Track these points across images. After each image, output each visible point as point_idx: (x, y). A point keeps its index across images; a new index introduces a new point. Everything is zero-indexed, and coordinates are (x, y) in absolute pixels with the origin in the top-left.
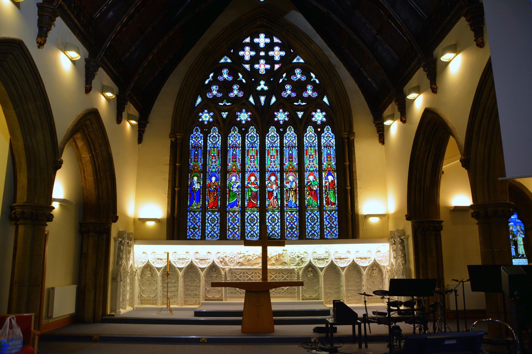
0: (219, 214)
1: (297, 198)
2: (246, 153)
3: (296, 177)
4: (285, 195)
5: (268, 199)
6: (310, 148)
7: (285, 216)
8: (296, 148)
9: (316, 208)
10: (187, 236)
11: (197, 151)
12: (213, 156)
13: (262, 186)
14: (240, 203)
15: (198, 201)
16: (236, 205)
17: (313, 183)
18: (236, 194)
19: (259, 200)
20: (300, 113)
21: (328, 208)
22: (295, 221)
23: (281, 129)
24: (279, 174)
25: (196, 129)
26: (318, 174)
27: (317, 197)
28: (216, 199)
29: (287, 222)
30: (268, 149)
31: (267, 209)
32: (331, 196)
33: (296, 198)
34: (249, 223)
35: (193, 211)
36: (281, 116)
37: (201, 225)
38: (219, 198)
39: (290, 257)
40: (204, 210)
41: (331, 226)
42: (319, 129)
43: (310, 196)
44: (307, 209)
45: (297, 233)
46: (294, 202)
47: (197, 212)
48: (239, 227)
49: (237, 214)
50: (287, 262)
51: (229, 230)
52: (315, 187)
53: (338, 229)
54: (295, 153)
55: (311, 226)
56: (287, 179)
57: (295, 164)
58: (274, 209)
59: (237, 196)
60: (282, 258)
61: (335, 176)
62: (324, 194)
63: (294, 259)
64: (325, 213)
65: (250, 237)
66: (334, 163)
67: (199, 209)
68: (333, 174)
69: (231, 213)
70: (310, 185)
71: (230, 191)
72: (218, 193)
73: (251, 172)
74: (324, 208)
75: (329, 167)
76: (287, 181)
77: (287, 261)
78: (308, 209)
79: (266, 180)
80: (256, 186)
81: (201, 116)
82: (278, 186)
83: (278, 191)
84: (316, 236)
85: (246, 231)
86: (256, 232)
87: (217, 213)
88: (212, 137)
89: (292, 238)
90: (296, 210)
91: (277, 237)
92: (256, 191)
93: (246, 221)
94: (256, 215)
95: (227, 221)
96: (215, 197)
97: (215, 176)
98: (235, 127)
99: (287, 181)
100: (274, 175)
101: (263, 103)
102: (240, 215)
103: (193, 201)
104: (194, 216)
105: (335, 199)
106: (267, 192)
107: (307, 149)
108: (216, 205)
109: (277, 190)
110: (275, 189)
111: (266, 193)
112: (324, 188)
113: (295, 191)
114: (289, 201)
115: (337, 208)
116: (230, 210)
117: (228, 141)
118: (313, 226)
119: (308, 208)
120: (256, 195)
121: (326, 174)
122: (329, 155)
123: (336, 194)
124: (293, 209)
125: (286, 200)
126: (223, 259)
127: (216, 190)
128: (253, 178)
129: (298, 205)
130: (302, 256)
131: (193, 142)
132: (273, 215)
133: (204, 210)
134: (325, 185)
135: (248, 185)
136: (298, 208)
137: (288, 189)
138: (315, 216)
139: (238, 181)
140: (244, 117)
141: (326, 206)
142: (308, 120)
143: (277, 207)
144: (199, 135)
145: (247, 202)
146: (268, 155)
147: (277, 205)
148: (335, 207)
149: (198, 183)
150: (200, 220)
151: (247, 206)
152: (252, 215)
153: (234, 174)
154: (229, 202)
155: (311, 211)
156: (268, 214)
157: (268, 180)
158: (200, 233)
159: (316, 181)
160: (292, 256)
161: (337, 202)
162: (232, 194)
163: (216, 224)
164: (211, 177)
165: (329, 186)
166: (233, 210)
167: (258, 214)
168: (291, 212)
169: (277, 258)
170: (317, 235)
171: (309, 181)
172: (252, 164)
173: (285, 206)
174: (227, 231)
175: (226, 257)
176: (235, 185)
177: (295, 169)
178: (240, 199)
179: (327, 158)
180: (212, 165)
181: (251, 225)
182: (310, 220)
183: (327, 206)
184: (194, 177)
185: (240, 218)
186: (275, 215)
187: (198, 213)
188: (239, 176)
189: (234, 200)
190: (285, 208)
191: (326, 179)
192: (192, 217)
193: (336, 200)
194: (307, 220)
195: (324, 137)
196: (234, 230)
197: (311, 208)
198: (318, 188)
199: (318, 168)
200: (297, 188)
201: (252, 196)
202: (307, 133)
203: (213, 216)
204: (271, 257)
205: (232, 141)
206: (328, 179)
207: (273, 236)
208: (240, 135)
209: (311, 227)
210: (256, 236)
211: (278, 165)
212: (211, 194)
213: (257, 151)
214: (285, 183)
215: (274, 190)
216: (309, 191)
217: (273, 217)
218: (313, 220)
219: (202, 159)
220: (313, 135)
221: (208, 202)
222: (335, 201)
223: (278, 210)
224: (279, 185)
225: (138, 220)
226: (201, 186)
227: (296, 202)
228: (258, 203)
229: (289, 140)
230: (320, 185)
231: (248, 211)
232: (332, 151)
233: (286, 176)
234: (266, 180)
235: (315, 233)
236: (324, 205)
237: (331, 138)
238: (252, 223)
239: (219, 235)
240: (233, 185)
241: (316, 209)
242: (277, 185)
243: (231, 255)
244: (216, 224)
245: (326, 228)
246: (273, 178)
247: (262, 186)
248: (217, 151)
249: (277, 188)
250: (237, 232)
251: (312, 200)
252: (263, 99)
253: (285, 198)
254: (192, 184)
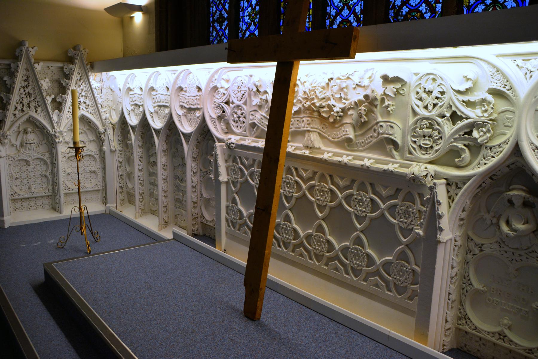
39: (415, 113)
50: (399, 141)
60: (380, 119)
63: (431, 126)
77: (404, 136)
126: (224, 112)
130: (474, 114)
160: (425, 113)
169: (361, 117)
175: (227, 103)
204: (343, 110)
225: (104, 11)
243: (239, 98)
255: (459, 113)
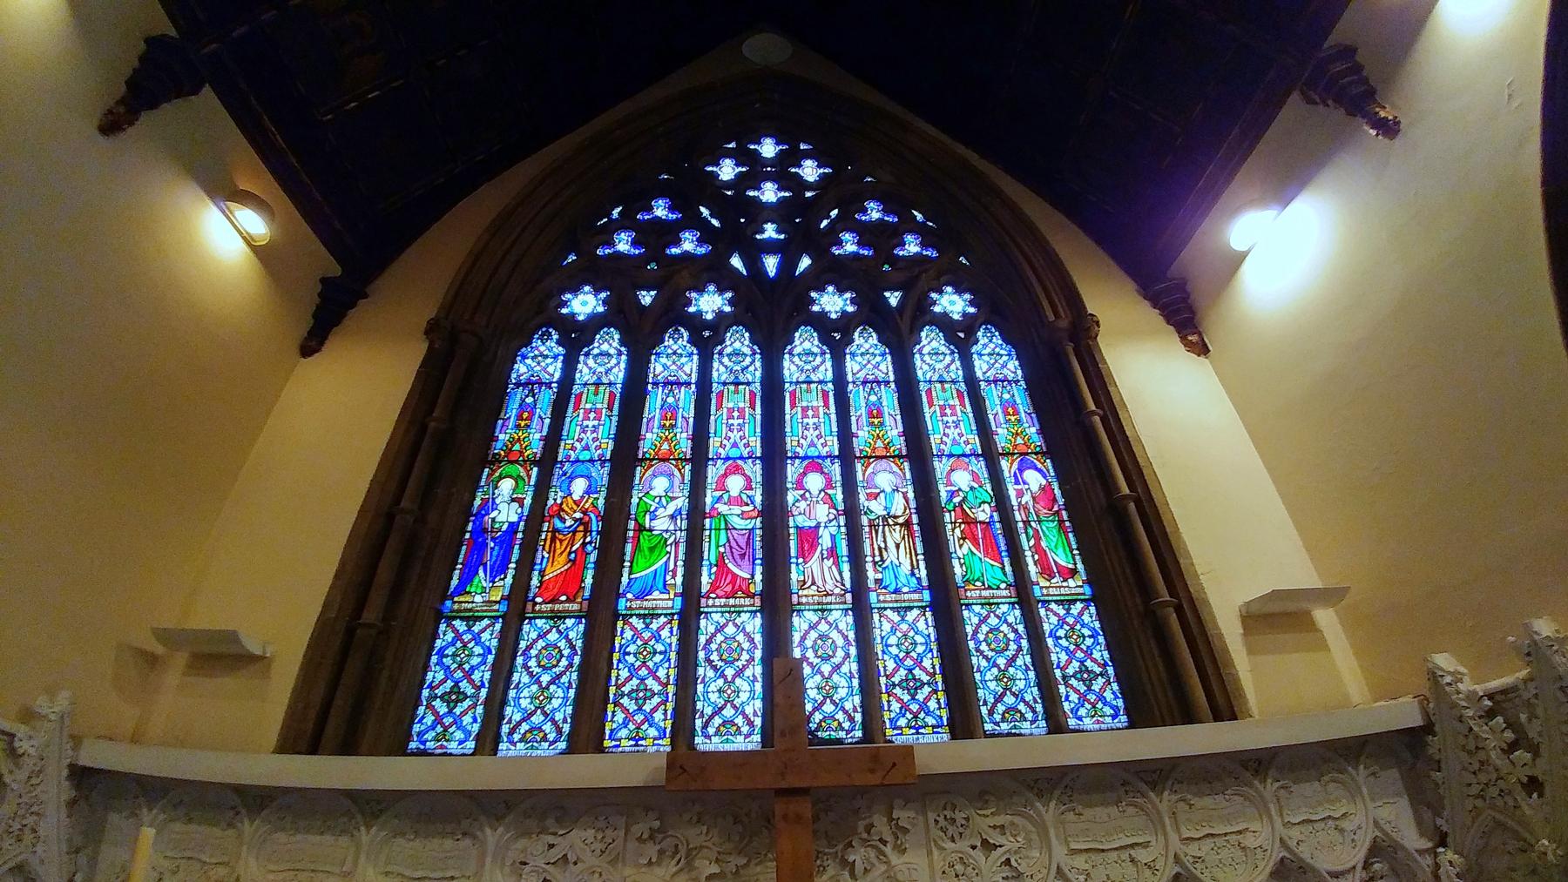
0: (582, 627)
1: (919, 552)
2: (714, 401)
3: (904, 474)
4: (868, 540)
5: (797, 558)
6: (938, 386)
7: (877, 632)
8: (893, 385)
9: (1005, 593)
10: (409, 738)
11: (534, 396)
12: (588, 412)
13: (774, 513)
14: (679, 579)
15: (499, 569)
16: (660, 585)
17: (970, 497)
18: (666, 540)
19: (761, 565)
20: (892, 293)
21: (1051, 591)
22: (920, 649)
23: (835, 336)
24: (837, 465)
25: (543, 335)
26: (983, 466)
27: (999, 547)
28: (577, 564)
29: (886, 657)
30: (791, 389)
31: (795, 599)
32: (1053, 545)
33: (912, 552)
34: (715, 668)
35: (467, 614)
36: (832, 302)
37: (490, 681)
38: (593, 557)
40: (517, 610)
41: (1083, 669)
42: (960, 336)
43: (968, 545)
44: (967, 598)
45: (940, 708)
46: (910, 568)
47: (482, 618)
48: (666, 685)
49: (665, 624)
51: (616, 704)
52: (983, 511)
53: (1118, 680)
54: (889, 399)
55: (995, 670)
56: (869, 483)
57: (895, 432)
58: (825, 600)
59: (668, 549)
61: (1048, 471)
62: (1023, 537)
64: (1042, 612)
65: (716, 734)
66: (1033, 430)
67: (496, 607)
68: (1039, 466)
69: (634, 620)
70: (960, 504)
71: (640, 529)
72: (588, 539)
73: (730, 462)
74: (1036, 588)
75: (1019, 441)
76: (868, 491)
78: (972, 598)
79: (788, 489)
80: (751, 508)
81: (569, 300)
82: (833, 506)
83: (839, 526)
84: (1025, 720)
85: (699, 705)
86: (749, 710)
87: (573, 620)
88: (597, 355)
89: (918, 733)
90: (922, 601)
91: (848, 732)
92: (750, 527)
93: (701, 655)
94: (749, 629)
95: (616, 656)
96: (573, 555)
97: (588, 477)
98: (679, 328)
99: (868, 491)
100: (819, 469)
101: (774, 271)
102: (675, 629)
103: (477, 573)
104: (467, 637)
105: (1070, 555)
106: (792, 531)
107: (930, 389)
108: (572, 591)
109: (834, 523)
110: (826, 519)
111: (789, 535)
112: (1017, 513)
113: (907, 524)
114: (887, 567)
115: (1087, 590)
116: (630, 608)
117: (652, 366)
118: (1006, 670)
119: (969, 594)
120: (748, 543)
121: (1015, 466)
122: (1009, 407)
123: (1071, 535)
124: (906, 597)
125: (875, 563)
127: (581, 528)
128: (735, 484)
129: (925, 583)
131: (523, 369)
132: (823, 627)
133: (517, 610)
134: (1020, 503)
135: (716, 506)
136: (926, 595)
137: (878, 518)
138: (1004, 628)
139: (675, 495)
140: (710, 303)
141: (1043, 583)
142: (919, 313)
143: (837, 591)
144: (551, 349)
145: (710, 575)
146: (793, 405)
147: (839, 584)
148: (1081, 587)
149: (513, 500)
150: (490, 658)
151: (710, 591)
152: (730, 630)
153: (664, 466)
154: (630, 574)
155: (982, 604)
156: (799, 623)
157: (796, 489)
158: (475, 720)
159: (979, 489)
161: (1080, 566)
162: (649, 541)
163: (562, 673)
164: (572, 478)
165: (1034, 507)
166: (645, 609)
167: (754, 624)
168: (903, 610)
170: (1029, 716)
171: (954, 489)
172: (735, 436)
173: (871, 584)
174: (610, 707)
176: (665, 508)
177: (894, 451)
178: (680, 563)
179: (1006, 413)
180: (580, 440)
181: (725, 677)
182: (989, 645)
183: (1048, 584)
184: (501, 478)
185: (673, 645)
186: (831, 625)
187: (486, 622)
188: (683, 476)
189: (654, 564)
190: (873, 597)
191: (1017, 482)
192: (453, 644)
193: (1078, 557)
194: (971, 644)
195: (980, 355)
196: (641, 702)
197: (980, 590)
198: (995, 514)
199: (978, 444)
200: (911, 514)
201: (731, 547)
202: (922, 344)
203: (553, 636)
205: (665, 367)
206: (1025, 483)
207: (829, 728)
208: (693, 348)
209: (997, 679)
210: (745, 729)
211: (831, 438)
212: (561, 541)
213: (752, 394)
214: (862, 497)
215: (819, 523)
216: (963, 526)
217: (823, 637)
218: (1002, 645)
219: (547, 421)
220: (943, 349)
221: (542, 573)
222: (1075, 564)
223: (845, 603)
224: (841, 507)
226: (522, 513)
227: (916, 571)
228: (758, 577)
229: (865, 362)
230: (1001, 501)
231: (710, 610)
232: (1016, 394)
233: (864, 475)
234: (788, 489)
235: (1022, 707)
236: (1034, 579)
237: (1005, 358)
238: (730, 663)
239: (566, 728)
240: (656, 510)
241: (1004, 597)
242: (833, 506)
244: (562, 673)
245: (1064, 677)
246: (814, 482)
247: (774, 513)
248: (607, 395)
249: (832, 517)
250: (655, 710)
251: (981, 559)
252: (771, 263)
253: (869, 553)
254: (489, 505)
255: (992, 841)
